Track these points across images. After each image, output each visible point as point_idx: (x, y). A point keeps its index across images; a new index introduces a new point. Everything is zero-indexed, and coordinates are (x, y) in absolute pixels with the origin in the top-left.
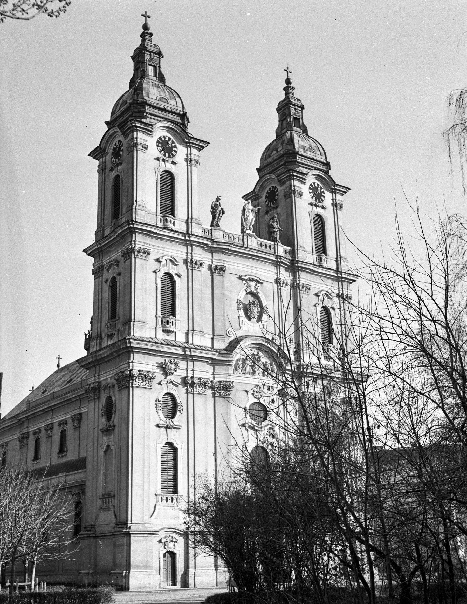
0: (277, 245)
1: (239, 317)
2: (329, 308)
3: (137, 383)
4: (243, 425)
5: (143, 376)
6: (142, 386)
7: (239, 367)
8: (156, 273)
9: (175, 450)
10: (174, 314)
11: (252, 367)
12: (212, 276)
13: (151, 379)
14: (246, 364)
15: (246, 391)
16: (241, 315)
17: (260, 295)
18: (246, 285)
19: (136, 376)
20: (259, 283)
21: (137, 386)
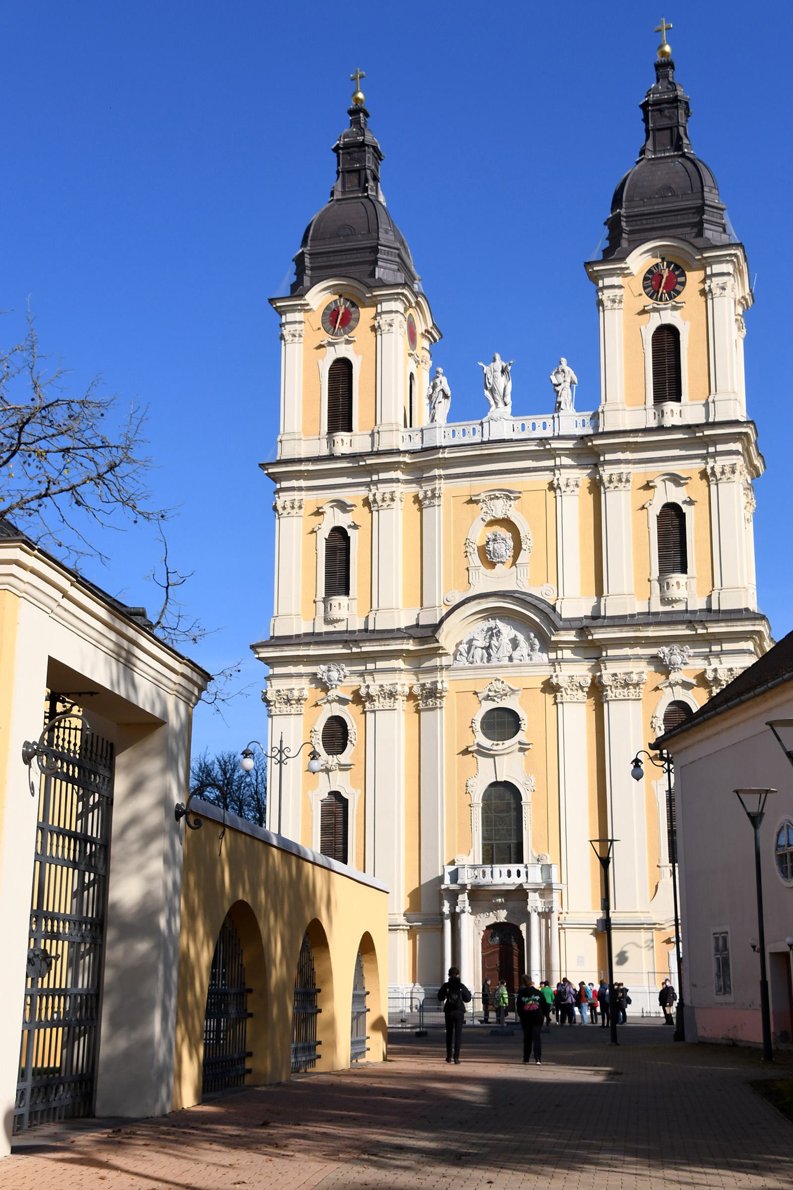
0: (558, 417)
1: (468, 569)
2: (680, 504)
3: (277, 710)
4: (466, 752)
5: (285, 697)
6: (285, 713)
7: (461, 654)
8: (316, 532)
9: (345, 802)
10: (345, 590)
11: (488, 648)
12: (421, 510)
13: (299, 700)
14: (473, 647)
15: (476, 693)
16: (472, 565)
17: (513, 519)
18: (484, 510)
19: (274, 699)
20: (511, 499)
21: (279, 713)
